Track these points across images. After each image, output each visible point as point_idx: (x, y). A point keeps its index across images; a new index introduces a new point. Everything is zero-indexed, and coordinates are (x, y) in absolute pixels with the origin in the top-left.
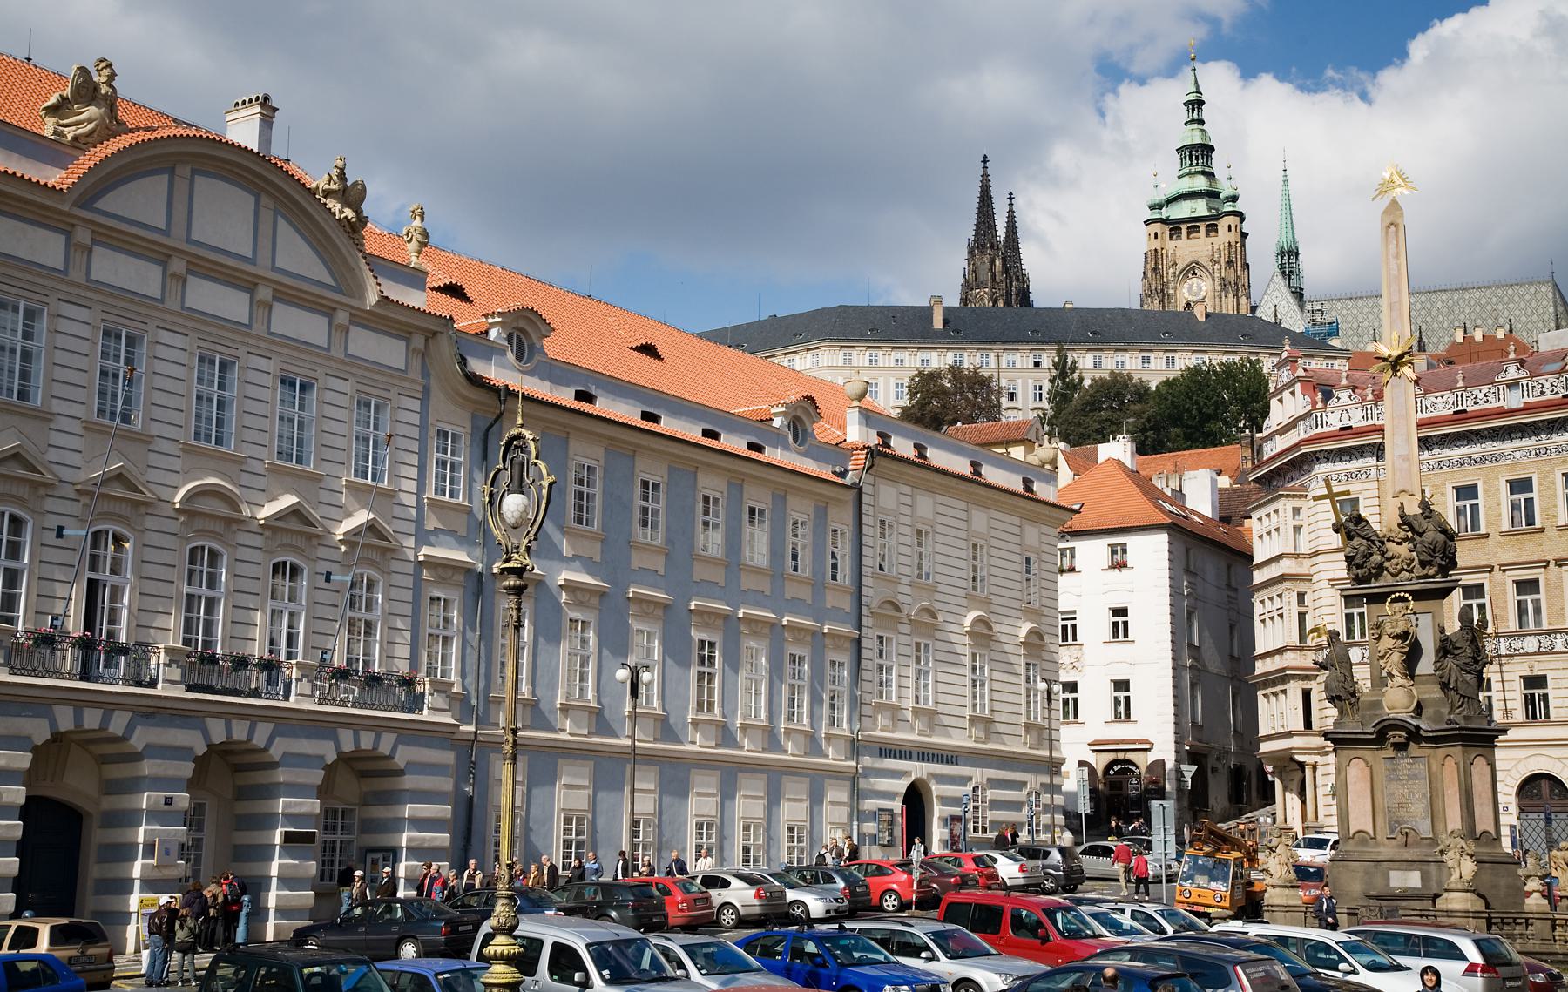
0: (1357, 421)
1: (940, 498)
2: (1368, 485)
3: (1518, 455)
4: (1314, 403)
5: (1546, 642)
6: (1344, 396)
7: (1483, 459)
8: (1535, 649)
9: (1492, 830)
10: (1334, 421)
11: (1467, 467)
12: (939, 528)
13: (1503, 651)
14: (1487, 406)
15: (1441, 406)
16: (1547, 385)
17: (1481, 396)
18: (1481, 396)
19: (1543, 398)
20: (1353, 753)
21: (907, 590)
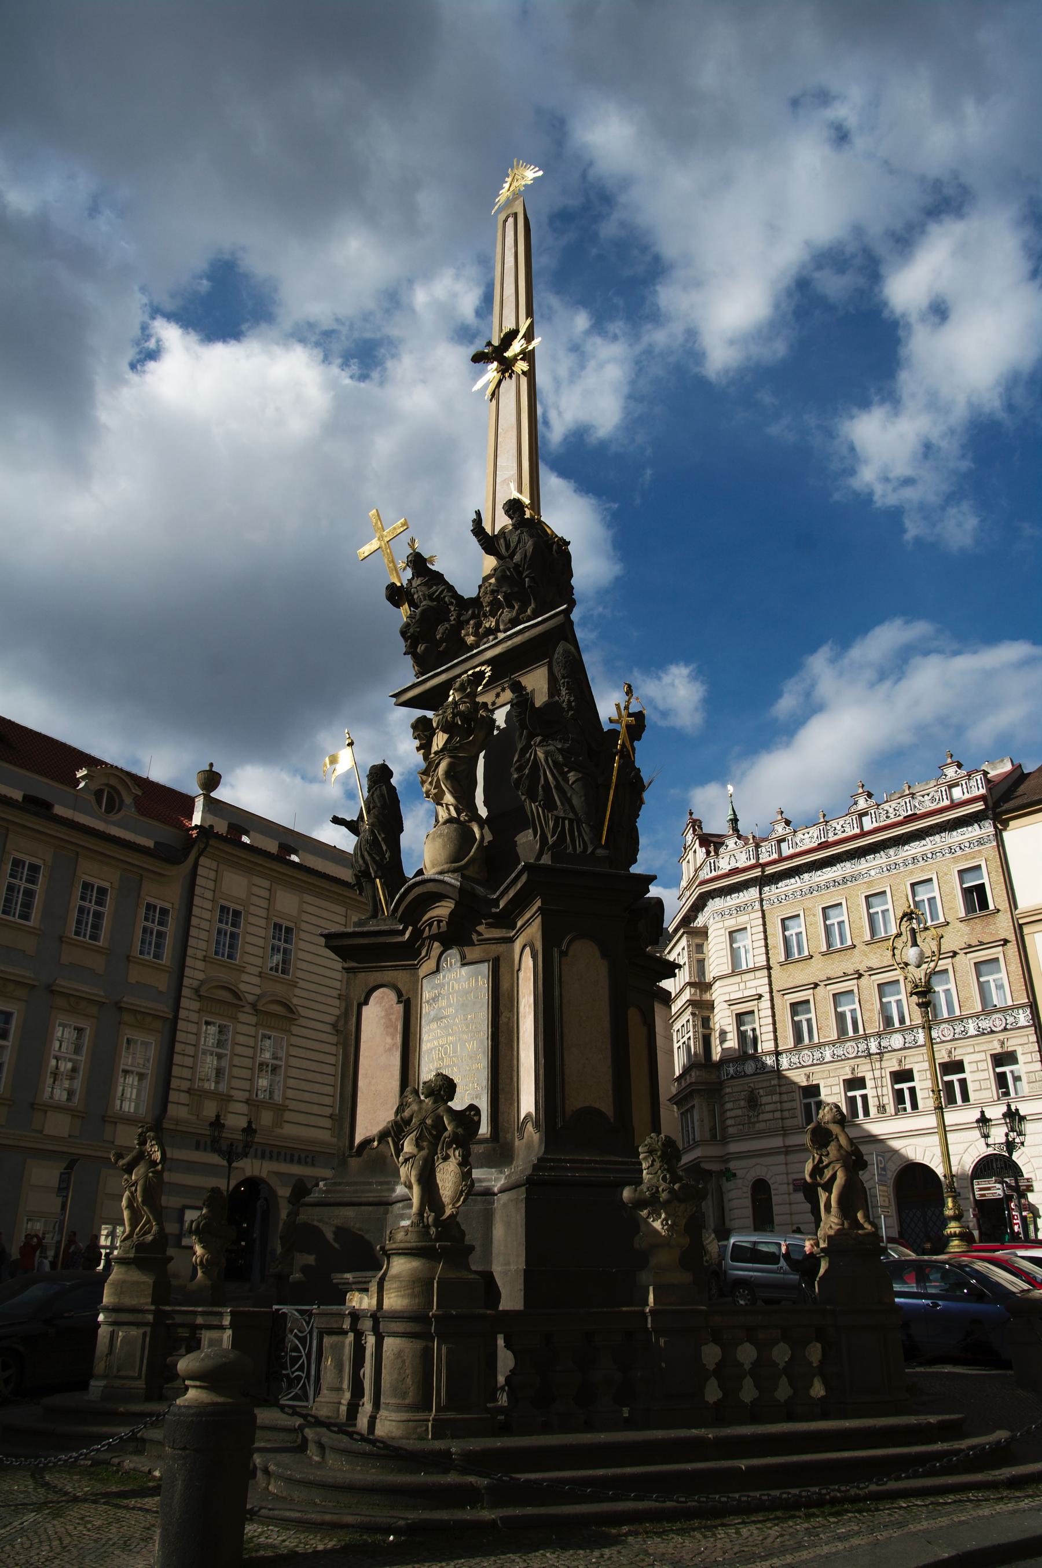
0: (742, 861)
1: (308, 898)
2: (753, 915)
3: (872, 873)
4: (708, 853)
5: (909, 1038)
6: (731, 843)
7: (845, 881)
8: (901, 1046)
9: (606, 1106)
10: (725, 864)
11: (832, 889)
12: (304, 926)
13: (874, 1049)
14: (844, 835)
15: (807, 841)
16: (891, 810)
17: (839, 827)
18: (839, 827)
19: (889, 821)
20: (374, 977)
21: (256, 980)
